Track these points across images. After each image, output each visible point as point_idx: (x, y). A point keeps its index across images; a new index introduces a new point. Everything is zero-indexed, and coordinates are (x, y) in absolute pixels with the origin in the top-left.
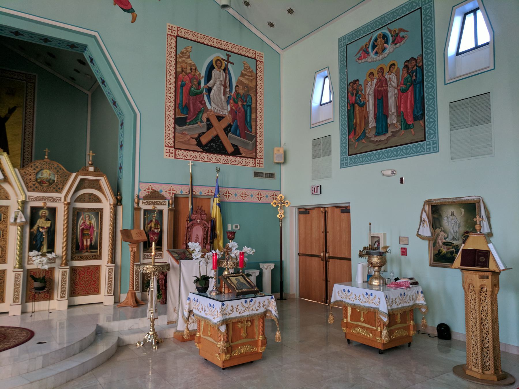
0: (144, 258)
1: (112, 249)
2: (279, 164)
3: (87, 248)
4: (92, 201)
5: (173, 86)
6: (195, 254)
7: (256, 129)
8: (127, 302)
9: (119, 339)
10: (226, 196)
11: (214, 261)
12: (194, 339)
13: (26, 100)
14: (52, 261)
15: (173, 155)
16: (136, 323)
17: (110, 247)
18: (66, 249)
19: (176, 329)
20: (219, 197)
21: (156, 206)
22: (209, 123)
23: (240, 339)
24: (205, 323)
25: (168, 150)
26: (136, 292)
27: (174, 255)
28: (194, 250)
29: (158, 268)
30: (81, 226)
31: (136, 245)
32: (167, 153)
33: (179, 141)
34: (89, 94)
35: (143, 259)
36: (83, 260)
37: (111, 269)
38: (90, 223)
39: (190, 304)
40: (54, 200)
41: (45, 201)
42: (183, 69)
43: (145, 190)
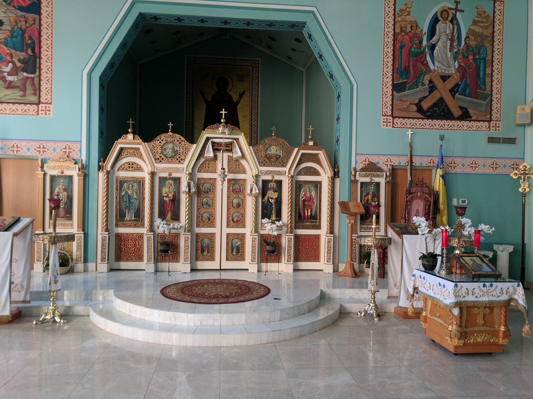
0: (361, 230)
1: (331, 220)
2: (524, 125)
3: (308, 219)
4: (312, 174)
5: (390, 50)
6: (421, 229)
7: (492, 86)
8: (346, 272)
9: (341, 306)
10: (451, 166)
11: (444, 237)
12: (419, 318)
13: (252, 84)
14: (280, 228)
15: (391, 124)
16: (357, 294)
18: (291, 218)
19: (398, 305)
20: (443, 168)
21: (373, 178)
22: (431, 85)
23: (476, 326)
24: (432, 303)
25: (385, 119)
26: (354, 263)
27: (395, 229)
28: (420, 225)
29: (379, 241)
30: (303, 198)
31: (354, 217)
32: (384, 122)
33: (397, 109)
34: (304, 70)
35: (360, 231)
36: (305, 229)
37: (330, 239)
38: (311, 195)
39: (414, 280)
40: (279, 173)
41: (273, 175)
42: (403, 29)
43: (362, 163)
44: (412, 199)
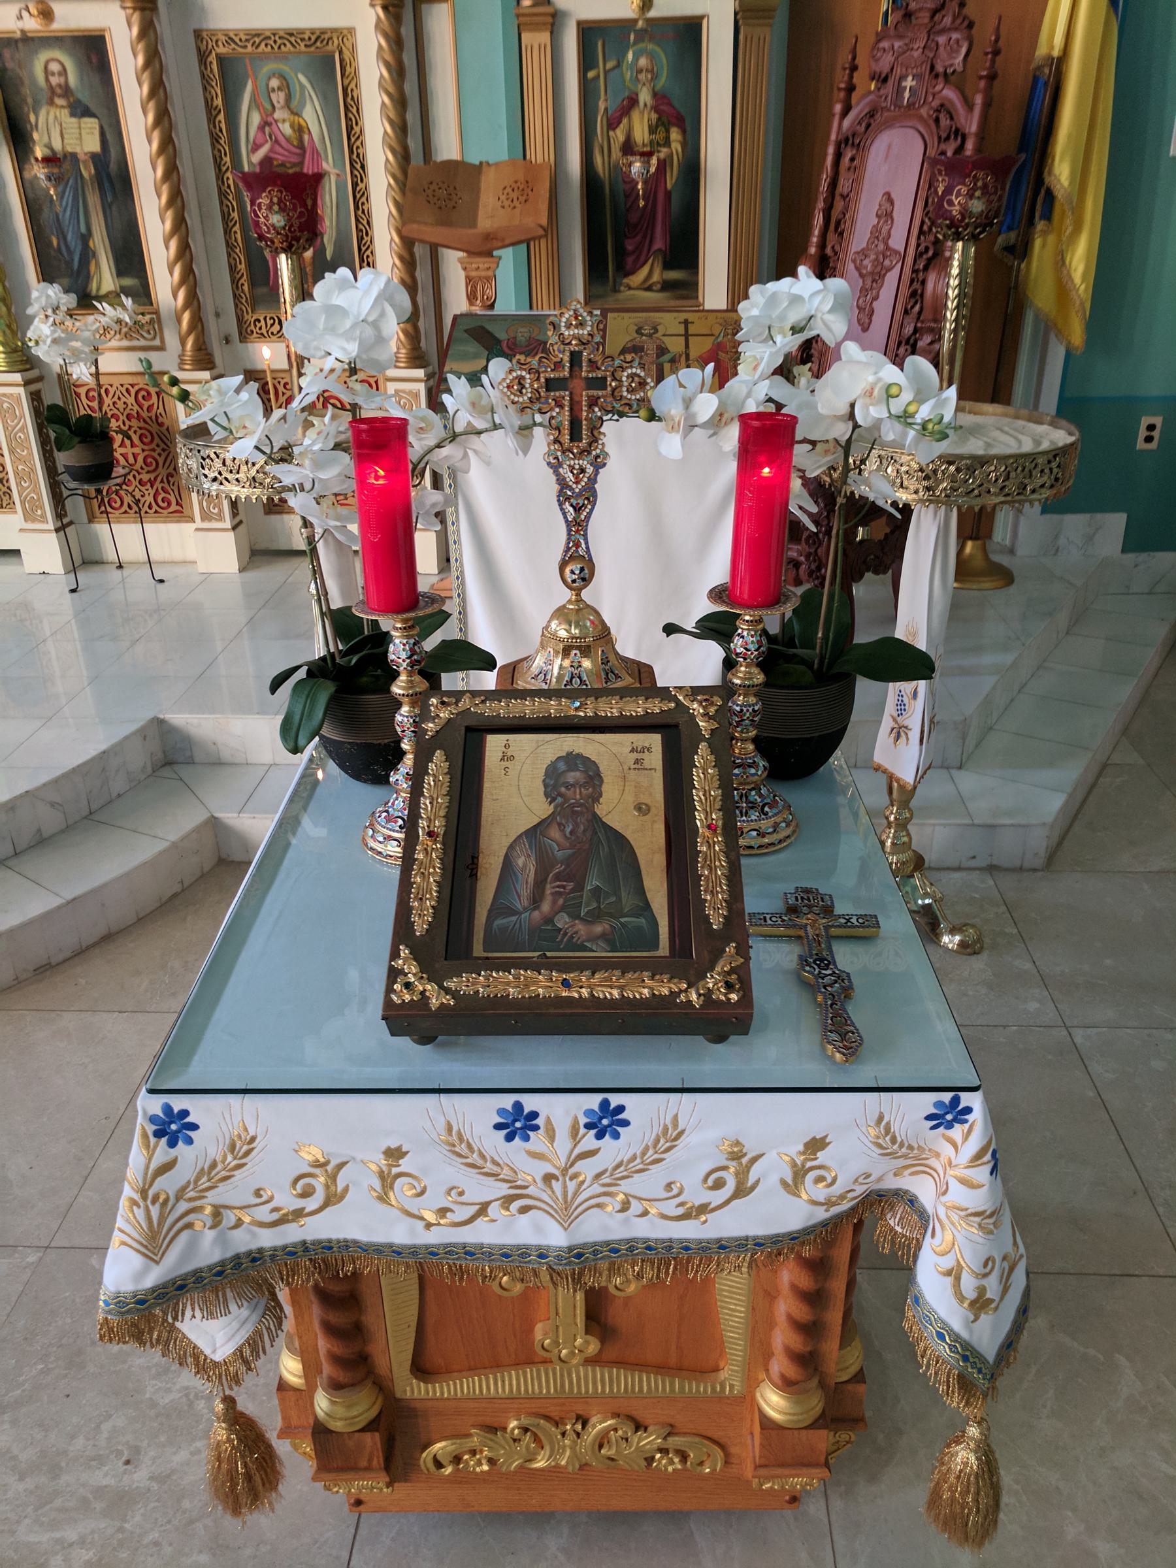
17: (395, 270)
30: (256, 147)
38: (300, 130)
44: (868, 126)
